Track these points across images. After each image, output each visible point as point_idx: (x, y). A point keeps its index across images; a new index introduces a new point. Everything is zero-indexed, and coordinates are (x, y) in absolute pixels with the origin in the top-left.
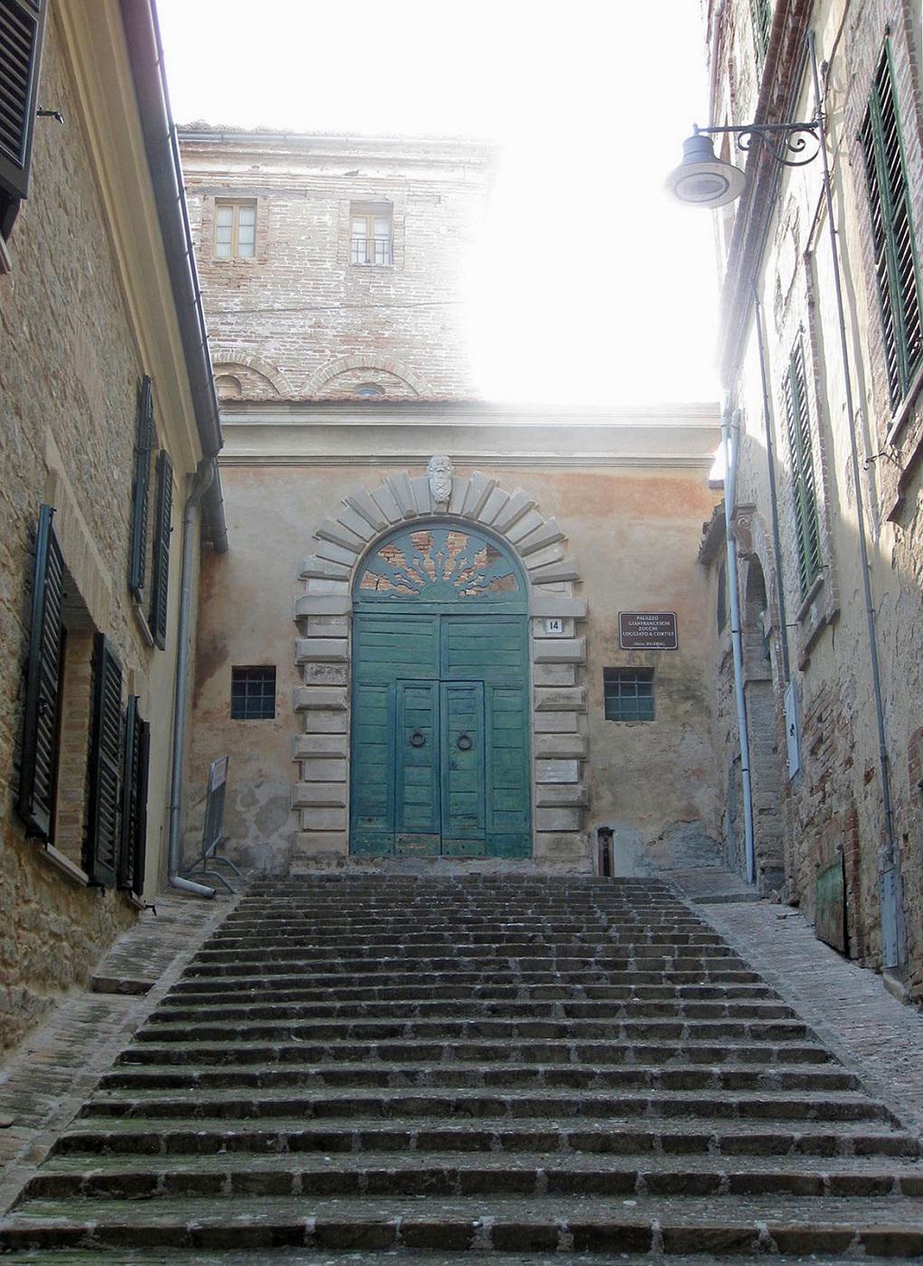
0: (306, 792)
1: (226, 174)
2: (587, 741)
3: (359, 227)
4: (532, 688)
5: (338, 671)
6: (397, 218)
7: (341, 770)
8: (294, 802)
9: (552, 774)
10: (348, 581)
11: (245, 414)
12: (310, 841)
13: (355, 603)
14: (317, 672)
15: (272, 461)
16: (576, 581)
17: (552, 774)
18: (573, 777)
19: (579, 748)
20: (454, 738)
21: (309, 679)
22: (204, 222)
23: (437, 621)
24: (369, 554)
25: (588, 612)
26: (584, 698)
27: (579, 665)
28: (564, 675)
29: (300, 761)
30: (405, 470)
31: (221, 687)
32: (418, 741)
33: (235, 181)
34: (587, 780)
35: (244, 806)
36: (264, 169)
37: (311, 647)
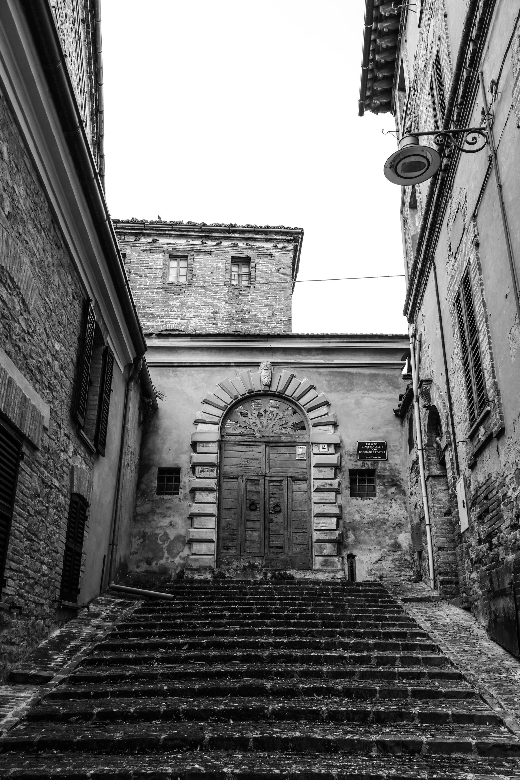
0: (195, 534)
1: (174, 244)
2: (341, 507)
3: (235, 269)
4: (312, 480)
5: (212, 471)
6: (252, 265)
7: (212, 522)
8: (187, 539)
9: (323, 525)
10: (218, 424)
11: (168, 341)
12: (196, 560)
13: (222, 436)
14: (201, 471)
15: (181, 365)
16: (335, 425)
17: (323, 525)
18: (334, 527)
19: (336, 511)
20: (272, 506)
21: (197, 474)
22: (164, 265)
23: (263, 446)
24: (229, 411)
25: (341, 441)
26: (340, 484)
27: (337, 468)
28: (329, 473)
29: (192, 517)
30: (248, 369)
31: (153, 481)
32: (253, 508)
33: (179, 247)
34: (341, 528)
35: (161, 541)
36: (191, 242)
37: (198, 458)
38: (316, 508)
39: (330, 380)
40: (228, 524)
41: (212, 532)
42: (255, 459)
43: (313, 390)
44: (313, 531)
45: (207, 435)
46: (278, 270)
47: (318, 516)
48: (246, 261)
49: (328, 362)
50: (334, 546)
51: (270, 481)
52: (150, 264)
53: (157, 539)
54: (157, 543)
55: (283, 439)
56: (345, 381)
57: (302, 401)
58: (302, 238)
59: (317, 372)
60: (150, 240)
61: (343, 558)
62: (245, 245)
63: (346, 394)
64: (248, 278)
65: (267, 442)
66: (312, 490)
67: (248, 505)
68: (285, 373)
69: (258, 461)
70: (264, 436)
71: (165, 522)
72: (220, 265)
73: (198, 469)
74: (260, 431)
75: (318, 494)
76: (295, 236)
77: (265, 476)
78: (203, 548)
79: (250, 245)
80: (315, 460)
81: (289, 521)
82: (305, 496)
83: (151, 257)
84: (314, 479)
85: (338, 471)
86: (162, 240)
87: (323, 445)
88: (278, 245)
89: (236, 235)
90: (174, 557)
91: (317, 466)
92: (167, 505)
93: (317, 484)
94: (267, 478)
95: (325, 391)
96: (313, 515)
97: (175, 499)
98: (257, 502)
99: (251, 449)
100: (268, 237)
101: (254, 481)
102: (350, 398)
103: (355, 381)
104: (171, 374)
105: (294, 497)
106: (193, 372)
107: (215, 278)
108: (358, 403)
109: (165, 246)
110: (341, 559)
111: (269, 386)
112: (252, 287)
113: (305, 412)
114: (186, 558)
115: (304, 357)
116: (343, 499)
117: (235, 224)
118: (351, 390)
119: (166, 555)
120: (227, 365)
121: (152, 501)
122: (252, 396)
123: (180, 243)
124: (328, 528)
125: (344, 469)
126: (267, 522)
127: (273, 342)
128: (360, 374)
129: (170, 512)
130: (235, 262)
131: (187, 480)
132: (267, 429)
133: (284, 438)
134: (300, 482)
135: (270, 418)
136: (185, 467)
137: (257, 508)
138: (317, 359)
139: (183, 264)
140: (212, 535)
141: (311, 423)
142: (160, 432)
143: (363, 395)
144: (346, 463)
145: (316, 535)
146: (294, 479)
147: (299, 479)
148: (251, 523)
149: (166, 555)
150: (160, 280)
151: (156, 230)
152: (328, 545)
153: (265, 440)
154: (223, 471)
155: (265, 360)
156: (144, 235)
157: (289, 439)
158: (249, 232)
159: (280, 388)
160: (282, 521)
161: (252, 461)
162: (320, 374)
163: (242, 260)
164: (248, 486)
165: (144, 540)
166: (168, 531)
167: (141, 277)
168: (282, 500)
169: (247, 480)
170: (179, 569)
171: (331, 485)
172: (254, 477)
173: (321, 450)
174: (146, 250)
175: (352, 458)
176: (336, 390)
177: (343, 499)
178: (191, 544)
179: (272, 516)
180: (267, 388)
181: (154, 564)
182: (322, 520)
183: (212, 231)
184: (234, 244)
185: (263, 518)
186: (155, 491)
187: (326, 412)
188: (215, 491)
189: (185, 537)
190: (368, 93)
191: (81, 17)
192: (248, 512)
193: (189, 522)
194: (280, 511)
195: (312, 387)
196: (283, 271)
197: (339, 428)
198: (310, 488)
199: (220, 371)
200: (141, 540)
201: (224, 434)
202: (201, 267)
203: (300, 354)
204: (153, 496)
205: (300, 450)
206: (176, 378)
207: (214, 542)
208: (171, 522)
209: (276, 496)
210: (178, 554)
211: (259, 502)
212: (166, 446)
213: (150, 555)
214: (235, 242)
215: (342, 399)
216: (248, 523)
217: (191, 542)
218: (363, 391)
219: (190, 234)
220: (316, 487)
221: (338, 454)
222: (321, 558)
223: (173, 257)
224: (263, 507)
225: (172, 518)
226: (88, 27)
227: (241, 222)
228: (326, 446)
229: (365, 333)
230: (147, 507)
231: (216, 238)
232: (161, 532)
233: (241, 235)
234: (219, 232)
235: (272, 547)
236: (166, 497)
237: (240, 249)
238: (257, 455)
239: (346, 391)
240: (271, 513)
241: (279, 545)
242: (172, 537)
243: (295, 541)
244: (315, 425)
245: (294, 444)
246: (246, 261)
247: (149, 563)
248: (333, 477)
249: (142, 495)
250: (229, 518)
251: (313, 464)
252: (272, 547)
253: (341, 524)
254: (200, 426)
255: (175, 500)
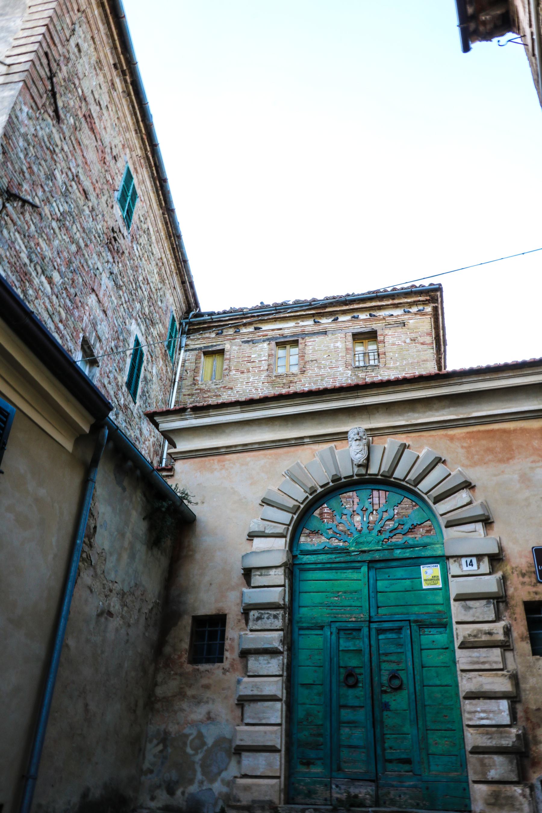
0: (247, 735)
1: (281, 329)
2: (515, 678)
3: (359, 348)
4: (455, 626)
5: (275, 617)
6: (380, 338)
7: (275, 713)
8: (234, 745)
9: (483, 715)
10: (285, 537)
11: (209, 416)
12: (247, 788)
13: (294, 557)
14: (259, 619)
15: (230, 450)
16: (487, 522)
17: (483, 715)
18: (505, 719)
19: (503, 684)
20: (385, 679)
21: (251, 625)
22: (269, 355)
23: (364, 569)
24: (304, 516)
25: (501, 549)
26: (507, 631)
27: (499, 600)
28: (483, 610)
29: (243, 702)
30: (332, 444)
31: (182, 637)
32: (351, 681)
33: (286, 332)
34: (521, 722)
35: (192, 749)
36: (302, 324)
37: (255, 596)
38: (464, 682)
39: (470, 447)
40: (308, 714)
41: (275, 732)
42: (351, 592)
43: (440, 465)
44: (465, 728)
45: (266, 555)
46: (413, 340)
47: (472, 696)
48: (371, 336)
49: (461, 416)
50: (511, 762)
51: (380, 631)
52: (253, 356)
53: (185, 744)
54: (185, 752)
55: (398, 553)
56: (498, 445)
57: (424, 486)
58: (442, 296)
59: (446, 435)
60: (251, 329)
61: (532, 788)
62: (368, 317)
63: (502, 466)
64: (376, 357)
65: (371, 562)
66: (457, 644)
67: (342, 677)
68: (391, 444)
69: (356, 595)
70: (364, 552)
71: (198, 713)
72: (339, 344)
73: (254, 614)
74: (357, 543)
75: (466, 652)
76: (432, 295)
77: (370, 622)
78: (259, 763)
79: (374, 316)
80: (456, 587)
81: (419, 707)
82: (444, 657)
83: (254, 349)
84: (458, 623)
85: (502, 606)
86: (265, 327)
87: (469, 560)
88: (410, 310)
89: (356, 306)
90: (212, 780)
91: (461, 598)
92: (205, 681)
93: (462, 632)
94: (374, 626)
95: (463, 466)
96: (462, 694)
97: (216, 669)
98: (357, 671)
99: (344, 576)
100: (396, 301)
101: (352, 631)
102: (511, 472)
103: (514, 442)
104: (216, 466)
105: (425, 659)
106: (248, 459)
107: (334, 361)
108: (525, 479)
109: (270, 333)
110: (528, 791)
111: (366, 465)
112: (381, 365)
113: (431, 503)
114: (229, 784)
115: (421, 415)
116: (519, 660)
117: (353, 294)
118: (508, 459)
119: (199, 776)
120: (299, 442)
121: (181, 675)
122: (338, 487)
123: (289, 328)
124: (493, 722)
125: (512, 603)
126: (378, 709)
127: (367, 396)
128: (523, 430)
129: (208, 694)
130: (359, 339)
131: (237, 635)
132: (370, 539)
133: (398, 551)
134: (433, 631)
135: (358, 517)
136: (233, 612)
137: (357, 682)
138: (443, 415)
139: (294, 351)
140: (275, 737)
141: (442, 521)
142: (198, 556)
143: (534, 465)
144: (516, 589)
145: (472, 739)
146: (422, 625)
147: (432, 625)
148: (349, 711)
149: (199, 776)
150: (266, 373)
151: (258, 316)
152: (498, 759)
153: (367, 557)
154: (296, 617)
155: (354, 427)
156: (245, 325)
157: (408, 553)
158: (371, 299)
159: (385, 467)
160: (405, 707)
161: (348, 596)
162: (452, 438)
163: (366, 336)
164: (341, 641)
165: (165, 747)
166: (204, 731)
167: (242, 373)
168: (402, 666)
169: (339, 630)
170: (220, 803)
171: (490, 633)
172: (350, 625)
173: (465, 568)
174: (247, 342)
175: (526, 579)
176: (482, 462)
177: (519, 660)
178: (240, 754)
179: (386, 698)
180: (363, 471)
181: (179, 792)
182: (481, 705)
183: (325, 306)
184: (354, 317)
185: (369, 702)
186: (185, 657)
187: (467, 500)
188: (281, 653)
189: (230, 741)
190: (470, 10)
191: (112, 62)
192: (344, 690)
193: (238, 712)
194: (400, 688)
195: (438, 461)
196: (421, 340)
197: (496, 526)
198: (452, 642)
199: (288, 452)
200: (160, 747)
201: (296, 553)
202: (314, 350)
203: (413, 410)
204: (181, 666)
205: (430, 573)
206: (223, 471)
207: (279, 751)
208: (209, 713)
209: (393, 658)
210: (219, 773)
211: (362, 671)
212: (207, 579)
213: (174, 775)
214: (356, 314)
215: (495, 475)
216: (343, 712)
217: (240, 750)
218: (532, 459)
219: (298, 314)
220: (461, 639)
221: (499, 574)
222: (484, 788)
223: (281, 345)
224: (368, 681)
225: (210, 706)
226: (124, 73)
227: (360, 288)
228: (474, 560)
229: (520, 359)
230: (173, 685)
231: (331, 314)
232: (192, 732)
233: (361, 306)
234: (334, 306)
235: (390, 761)
236: (203, 667)
237: (363, 322)
238: (355, 585)
239: (501, 461)
240: (385, 692)
241: (404, 756)
242: (210, 741)
243: (433, 749)
244: (449, 525)
245: (417, 561)
246: (371, 336)
247: (171, 792)
248: (492, 617)
249: (166, 666)
250: (310, 702)
251: (452, 596)
252: (390, 761)
253: (520, 714)
254: (256, 540)
255: (216, 672)
